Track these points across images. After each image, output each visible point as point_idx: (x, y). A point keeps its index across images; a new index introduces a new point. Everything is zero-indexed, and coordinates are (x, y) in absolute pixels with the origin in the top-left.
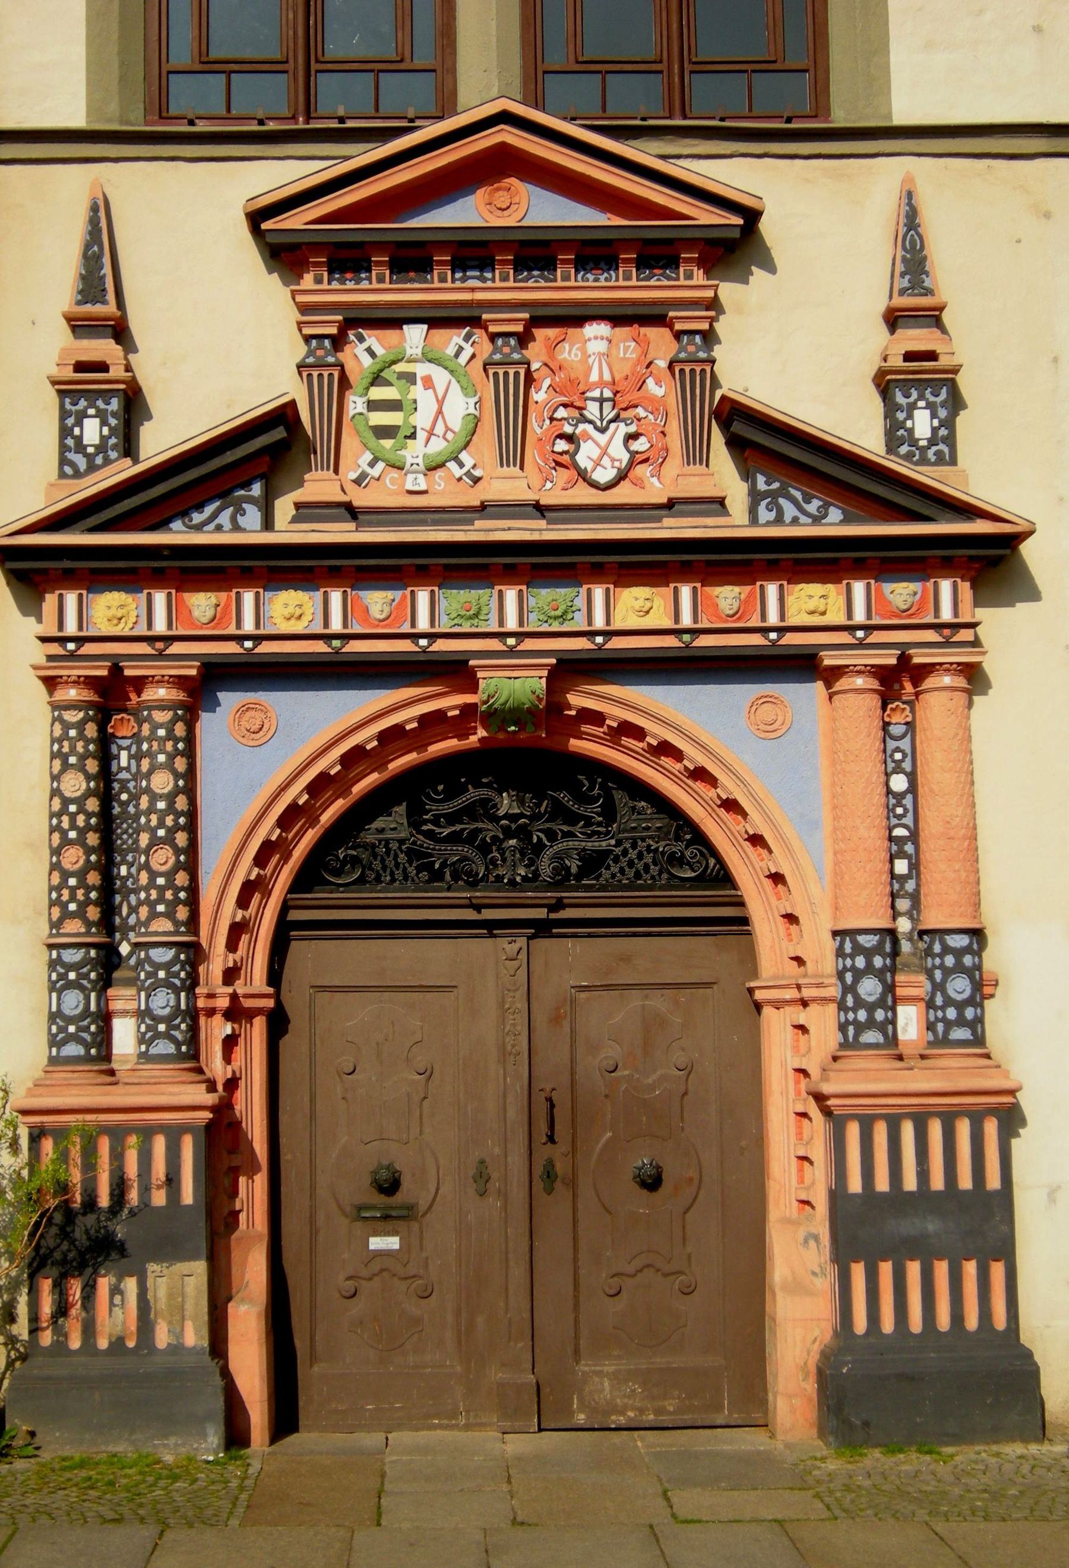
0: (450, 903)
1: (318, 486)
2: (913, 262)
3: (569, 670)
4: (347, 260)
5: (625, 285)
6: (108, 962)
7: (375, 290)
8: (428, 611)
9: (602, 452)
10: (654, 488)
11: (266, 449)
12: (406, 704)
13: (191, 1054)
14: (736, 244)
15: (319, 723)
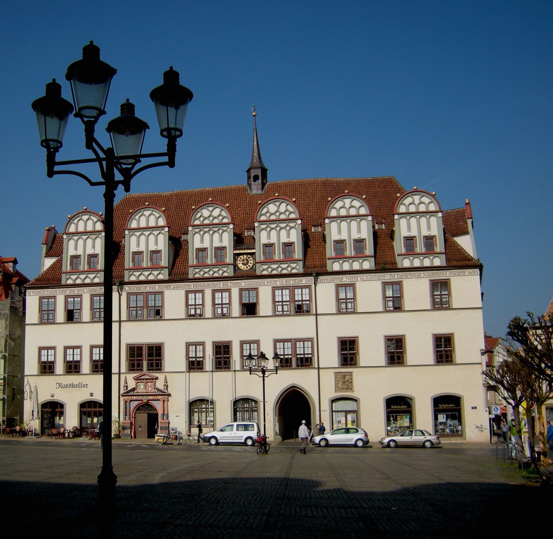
0: (144, 412)
1: (136, 391)
2: (166, 379)
3: (148, 400)
4: (137, 380)
5: (151, 381)
6: (126, 415)
7: (139, 381)
8: (141, 398)
9: (150, 389)
10: (152, 391)
11: (134, 389)
12: (141, 402)
13: (130, 419)
14: (157, 378)
15: (136, 403)
